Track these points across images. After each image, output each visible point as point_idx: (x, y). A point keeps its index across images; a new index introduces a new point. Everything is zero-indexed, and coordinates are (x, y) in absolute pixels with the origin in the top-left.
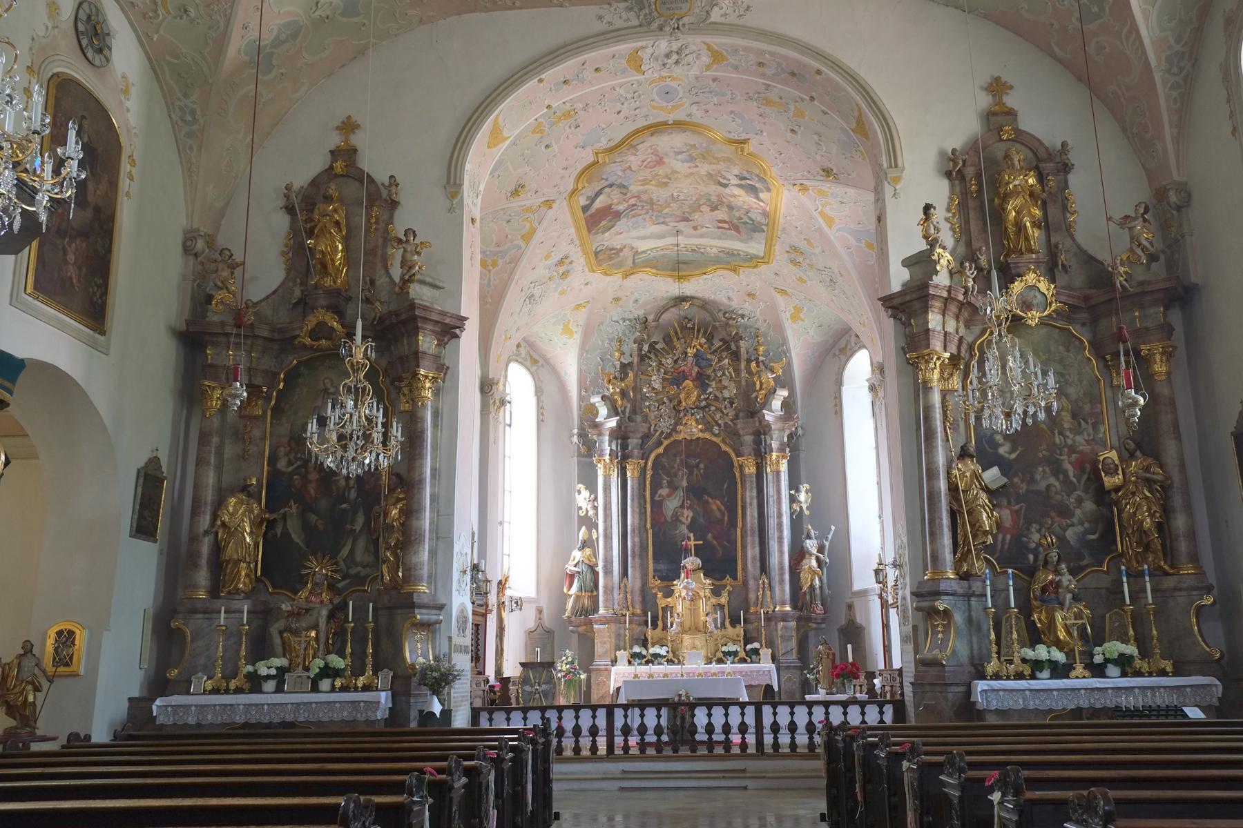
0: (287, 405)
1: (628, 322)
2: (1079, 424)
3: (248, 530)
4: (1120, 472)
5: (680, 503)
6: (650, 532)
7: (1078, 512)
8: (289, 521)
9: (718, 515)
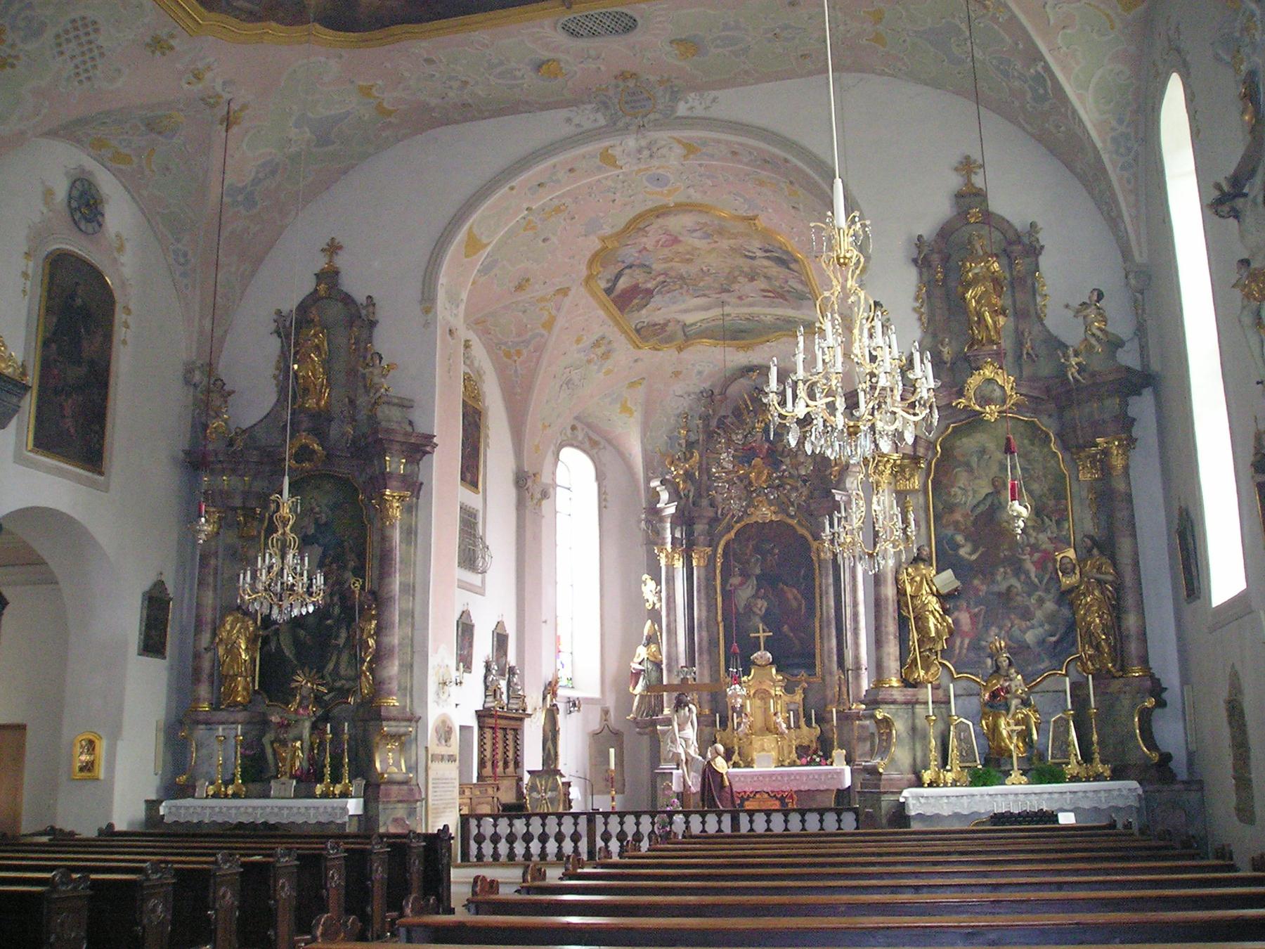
1: (693, 396)
2: (1043, 521)
3: (243, 647)
4: (1077, 571)
5: (754, 592)
6: (721, 625)
7: (1039, 614)
9: (795, 604)
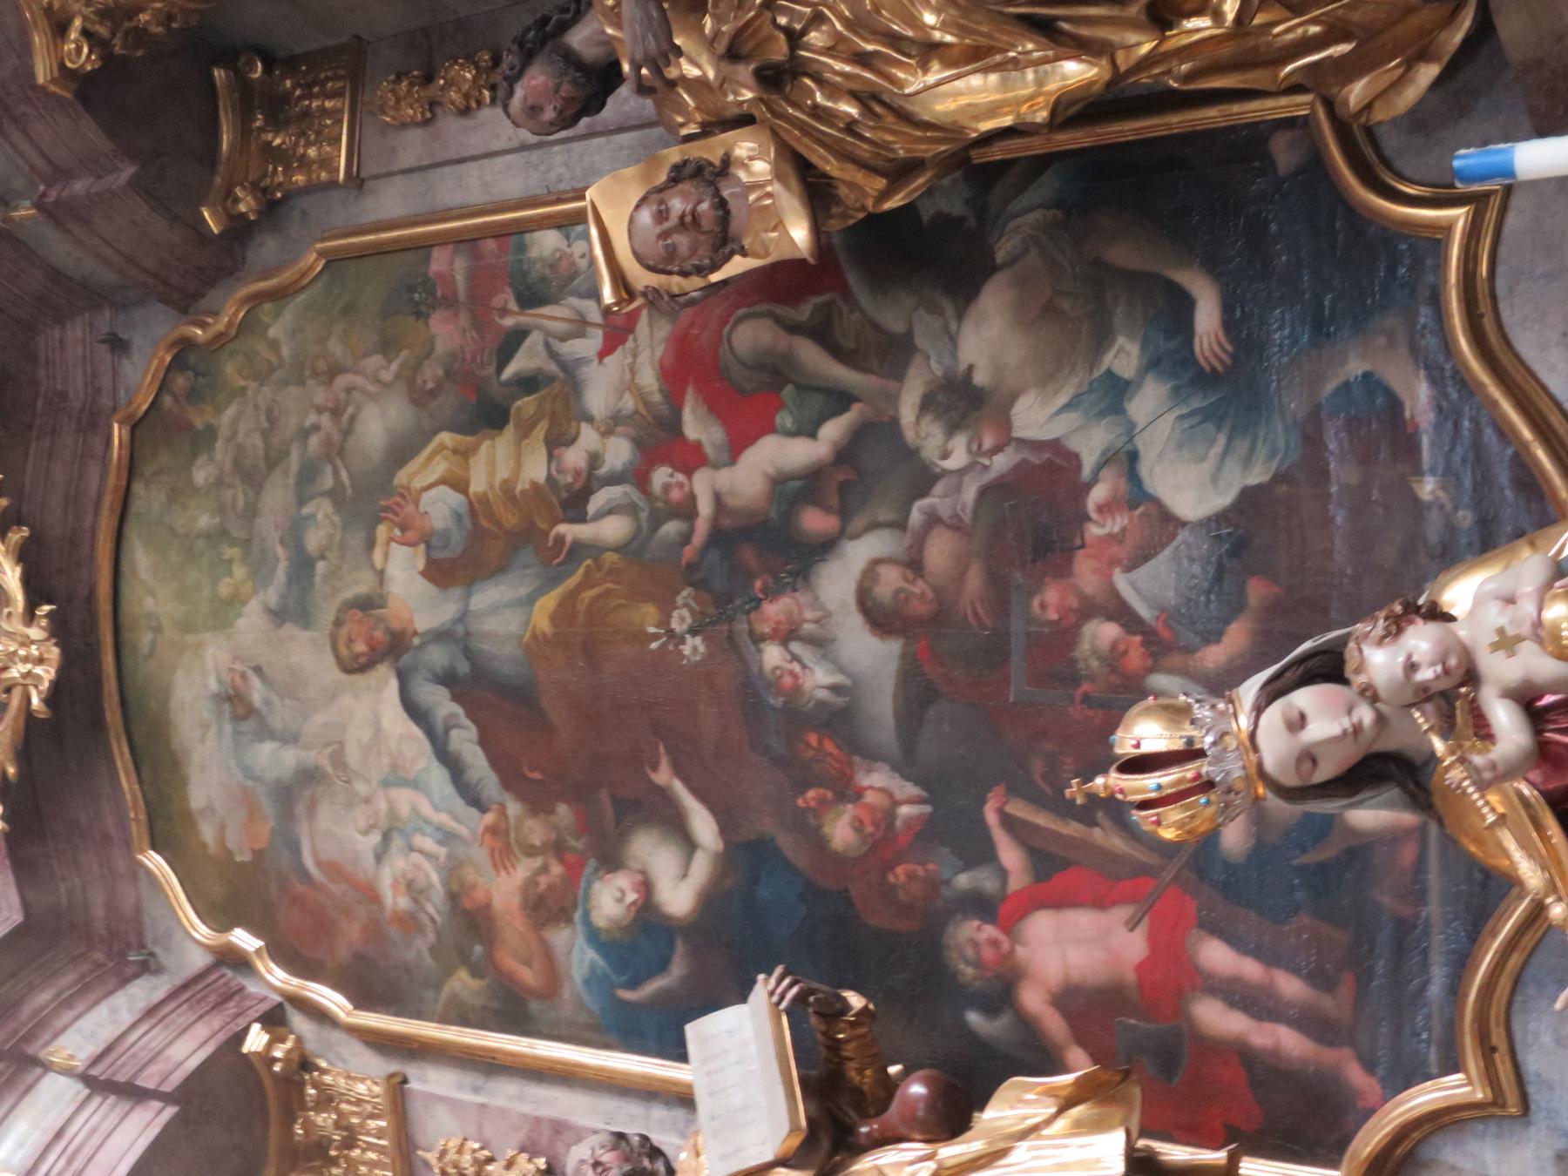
2: (529, 383)
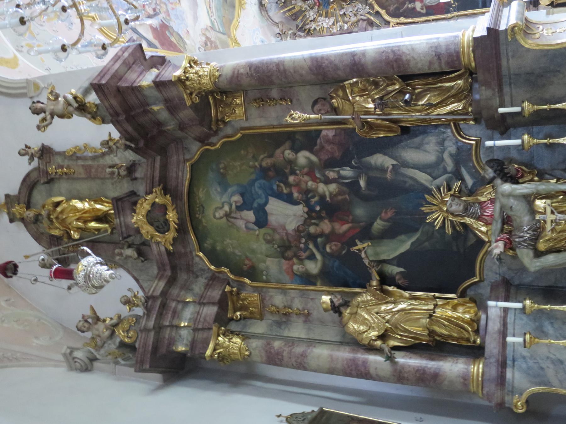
0: (247, 262)
3: (390, 307)
8: (383, 257)
